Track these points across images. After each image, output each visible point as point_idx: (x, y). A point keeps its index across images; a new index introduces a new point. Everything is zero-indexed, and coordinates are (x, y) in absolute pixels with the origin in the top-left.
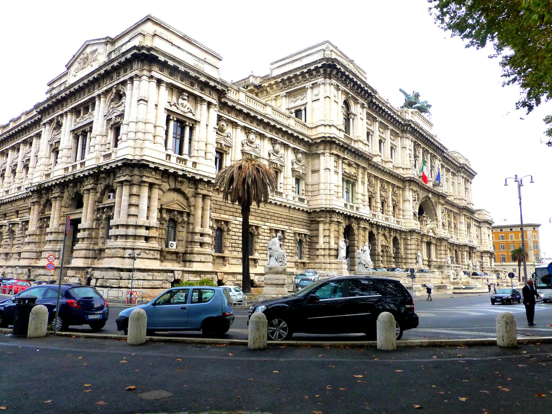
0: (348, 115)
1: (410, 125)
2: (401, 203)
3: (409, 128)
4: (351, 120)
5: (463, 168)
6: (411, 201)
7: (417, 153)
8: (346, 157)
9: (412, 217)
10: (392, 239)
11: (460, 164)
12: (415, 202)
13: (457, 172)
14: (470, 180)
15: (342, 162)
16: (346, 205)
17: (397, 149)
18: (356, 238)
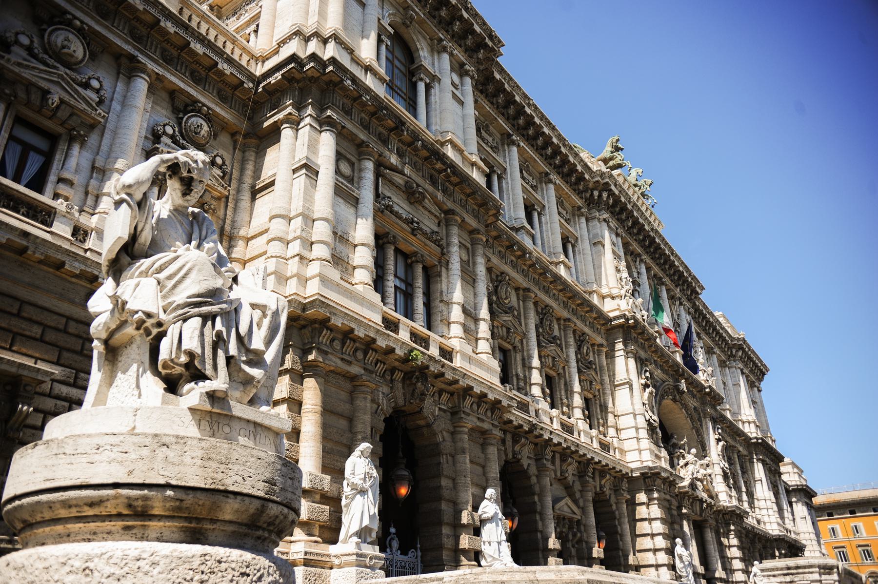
0: (412, 74)
1: (606, 187)
2: (608, 392)
3: (605, 195)
4: (421, 87)
5: (740, 348)
6: (636, 386)
7: (635, 275)
8: (394, 160)
9: (643, 434)
10: (590, 496)
11: (732, 339)
12: (648, 390)
13: (729, 359)
14: (757, 384)
15: (378, 175)
16: (391, 325)
17: (580, 246)
18: (447, 469)
